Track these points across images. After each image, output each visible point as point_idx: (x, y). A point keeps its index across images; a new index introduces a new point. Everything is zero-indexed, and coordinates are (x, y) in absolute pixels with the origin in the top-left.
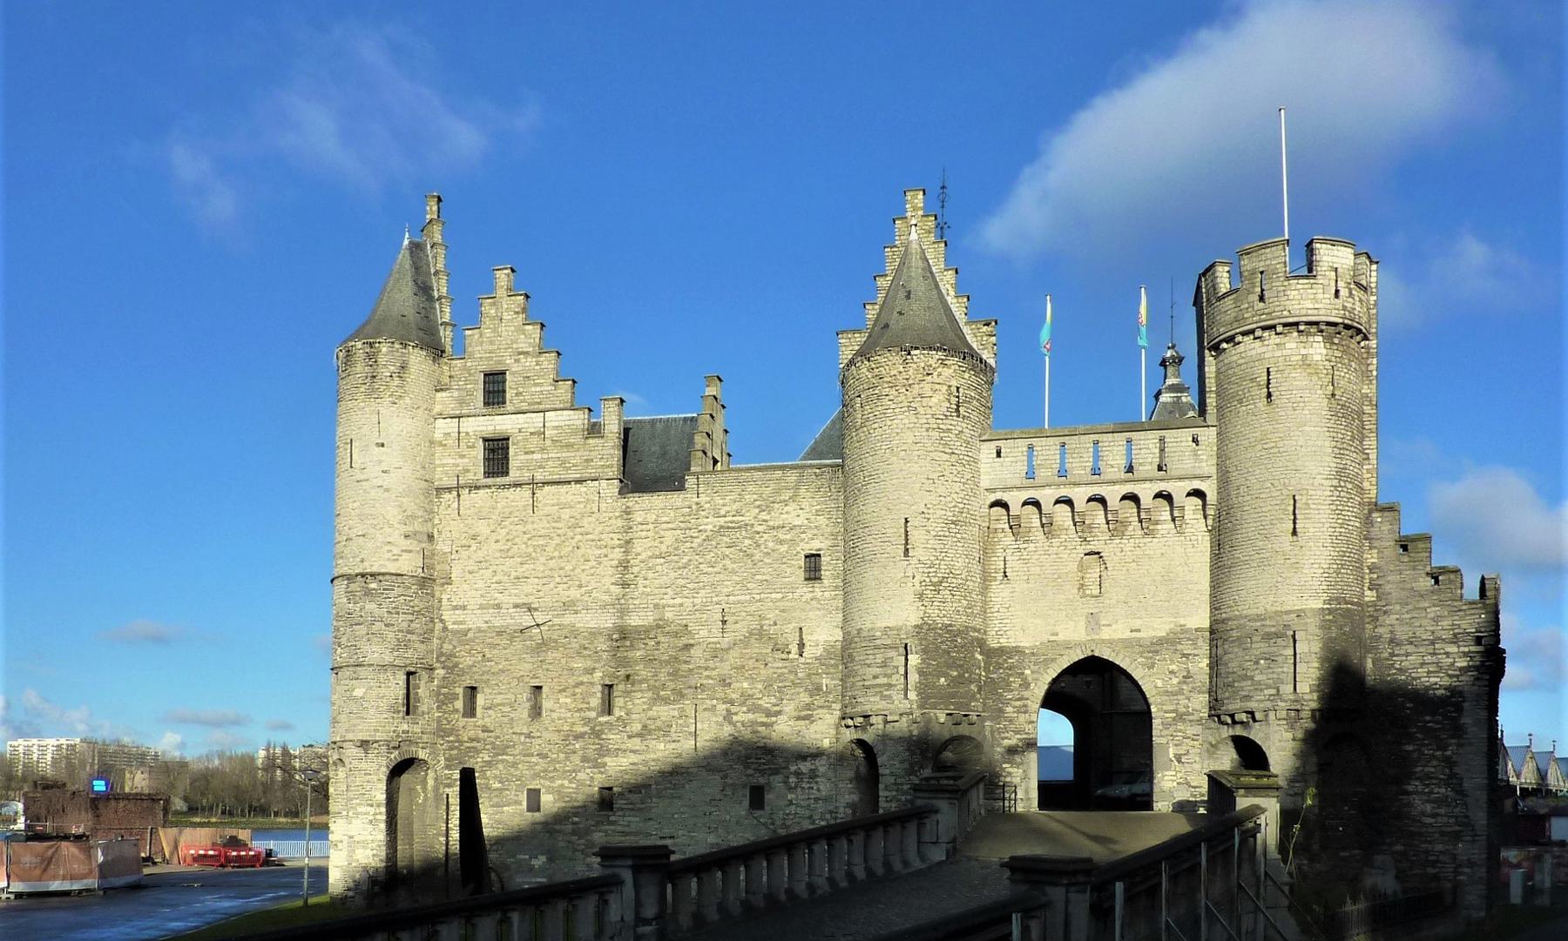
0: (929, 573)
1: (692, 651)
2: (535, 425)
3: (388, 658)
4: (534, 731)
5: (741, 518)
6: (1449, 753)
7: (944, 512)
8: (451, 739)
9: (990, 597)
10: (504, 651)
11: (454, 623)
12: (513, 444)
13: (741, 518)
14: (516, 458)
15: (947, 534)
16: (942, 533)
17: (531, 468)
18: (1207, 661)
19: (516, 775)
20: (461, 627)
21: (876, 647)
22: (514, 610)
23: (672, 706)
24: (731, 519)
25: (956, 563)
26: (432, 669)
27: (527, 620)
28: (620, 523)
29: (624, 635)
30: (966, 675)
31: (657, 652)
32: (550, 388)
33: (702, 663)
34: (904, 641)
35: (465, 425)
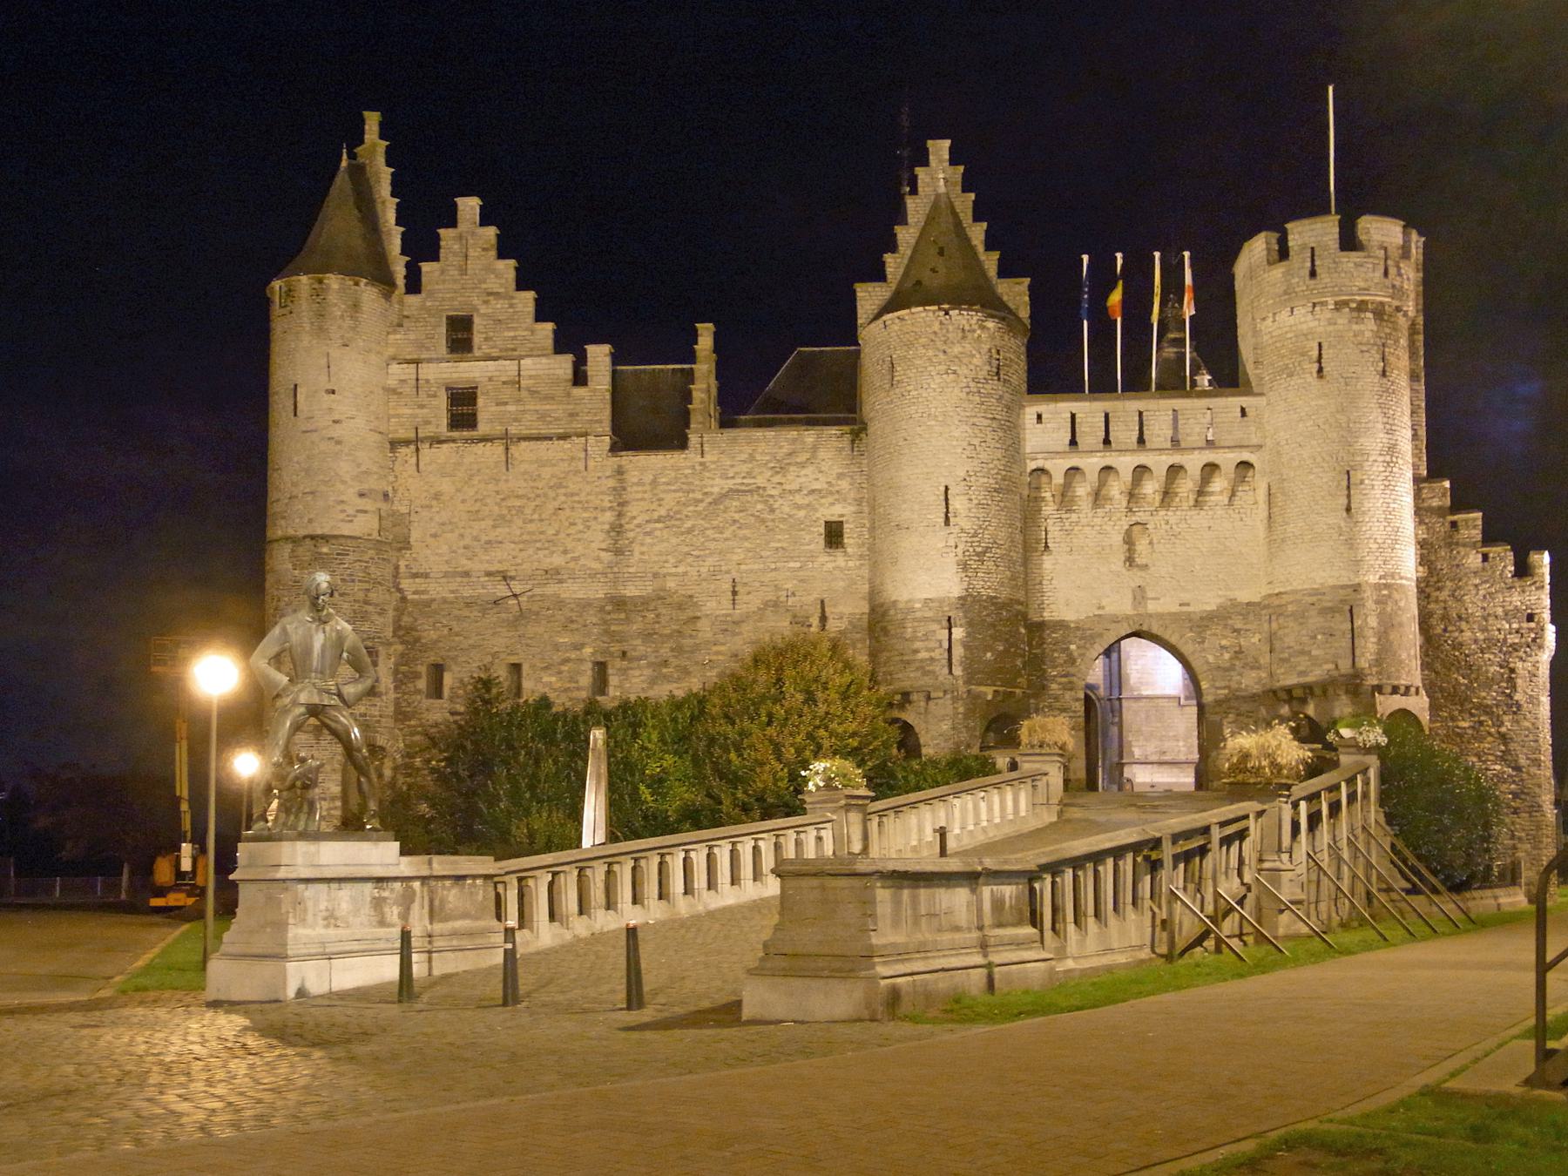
0: (972, 542)
1: (699, 624)
2: (509, 373)
5: (752, 481)
6: (1503, 729)
7: (986, 480)
8: (412, 723)
11: (415, 593)
12: (483, 394)
13: (752, 481)
14: (485, 409)
15: (990, 502)
16: (985, 502)
18: (1257, 637)
20: (422, 597)
22: (487, 579)
24: (740, 481)
26: (390, 644)
27: (501, 590)
28: (611, 483)
29: (619, 603)
30: (1013, 650)
31: (657, 626)
32: (525, 333)
33: (709, 635)
35: (425, 371)
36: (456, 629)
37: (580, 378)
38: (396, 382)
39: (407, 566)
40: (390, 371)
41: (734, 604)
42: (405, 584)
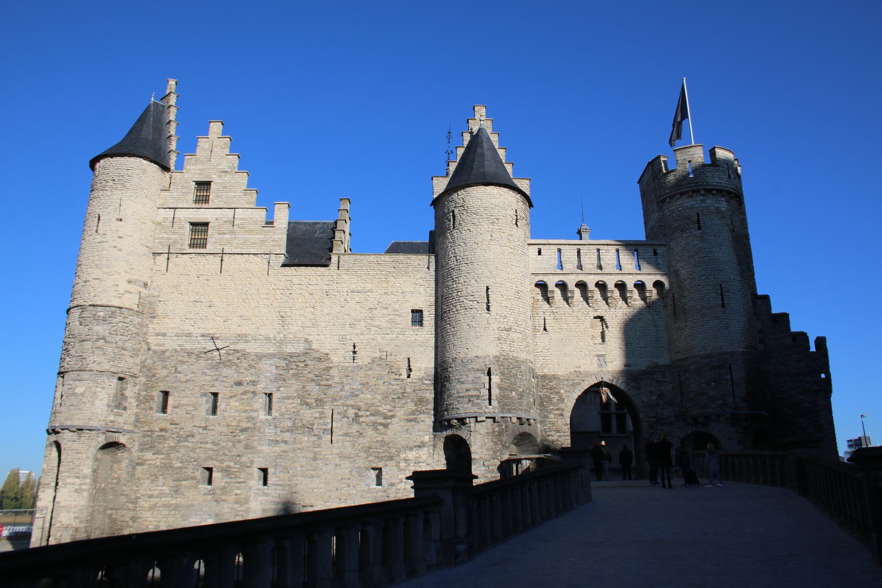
1: (332, 372)
3: (106, 366)
4: (210, 425)
9: (536, 342)
10: (192, 367)
11: (156, 345)
17: (222, 243)
19: (194, 458)
20: (161, 348)
21: (469, 370)
22: (202, 338)
23: (315, 410)
25: (519, 317)
27: (210, 346)
31: (306, 372)
32: (240, 194)
33: (337, 380)
34: (488, 367)
36: (179, 369)
37: (270, 223)
38: (162, 219)
39: (153, 328)
40: (159, 213)
41: (354, 360)
42: (151, 340)
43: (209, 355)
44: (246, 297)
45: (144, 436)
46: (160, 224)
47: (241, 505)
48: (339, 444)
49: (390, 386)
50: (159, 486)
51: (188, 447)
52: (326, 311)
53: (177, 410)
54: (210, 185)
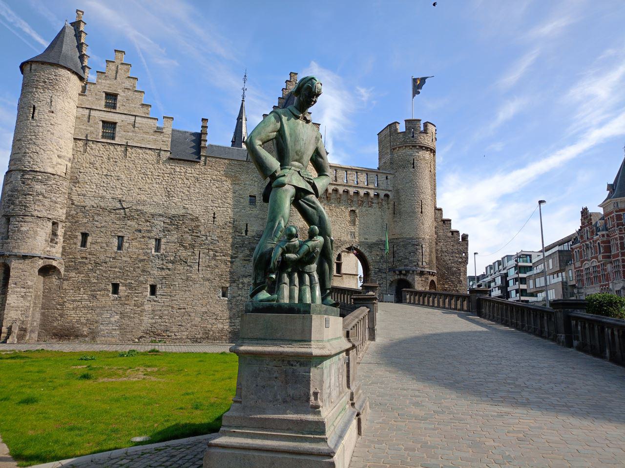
3: (44, 214)
27: (119, 206)
33: (203, 233)
41: (214, 222)
43: (117, 211)
44: (144, 176)
45: (69, 262)
46: (79, 118)
47: (138, 307)
48: (203, 272)
49: (235, 240)
50: (80, 294)
51: (102, 270)
52: (197, 191)
53: (94, 246)
54: (117, 96)
